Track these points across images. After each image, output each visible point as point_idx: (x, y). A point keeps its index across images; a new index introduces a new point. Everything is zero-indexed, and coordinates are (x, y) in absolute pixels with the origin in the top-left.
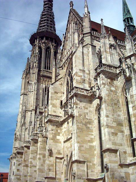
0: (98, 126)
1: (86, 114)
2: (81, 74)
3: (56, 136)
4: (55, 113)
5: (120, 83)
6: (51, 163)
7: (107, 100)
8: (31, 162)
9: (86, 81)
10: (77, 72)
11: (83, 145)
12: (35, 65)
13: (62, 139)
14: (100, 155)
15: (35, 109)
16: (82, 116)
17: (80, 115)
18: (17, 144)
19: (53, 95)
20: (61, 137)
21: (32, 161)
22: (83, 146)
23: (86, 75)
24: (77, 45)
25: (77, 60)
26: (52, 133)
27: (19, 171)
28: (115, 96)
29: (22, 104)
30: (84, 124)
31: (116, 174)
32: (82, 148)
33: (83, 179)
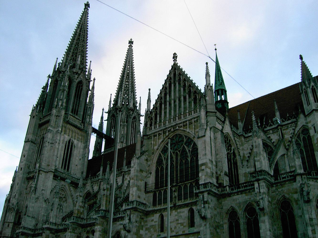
0: (228, 232)
1: (216, 216)
2: (210, 165)
4: (140, 198)
5: (275, 193)
10: (208, 162)
12: (60, 103)
13: (146, 234)
17: (212, 217)
18: (12, 217)
19: (139, 174)
23: (214, 168)
24: (205, 127)
25: (207, 147)
29: (26, 156)
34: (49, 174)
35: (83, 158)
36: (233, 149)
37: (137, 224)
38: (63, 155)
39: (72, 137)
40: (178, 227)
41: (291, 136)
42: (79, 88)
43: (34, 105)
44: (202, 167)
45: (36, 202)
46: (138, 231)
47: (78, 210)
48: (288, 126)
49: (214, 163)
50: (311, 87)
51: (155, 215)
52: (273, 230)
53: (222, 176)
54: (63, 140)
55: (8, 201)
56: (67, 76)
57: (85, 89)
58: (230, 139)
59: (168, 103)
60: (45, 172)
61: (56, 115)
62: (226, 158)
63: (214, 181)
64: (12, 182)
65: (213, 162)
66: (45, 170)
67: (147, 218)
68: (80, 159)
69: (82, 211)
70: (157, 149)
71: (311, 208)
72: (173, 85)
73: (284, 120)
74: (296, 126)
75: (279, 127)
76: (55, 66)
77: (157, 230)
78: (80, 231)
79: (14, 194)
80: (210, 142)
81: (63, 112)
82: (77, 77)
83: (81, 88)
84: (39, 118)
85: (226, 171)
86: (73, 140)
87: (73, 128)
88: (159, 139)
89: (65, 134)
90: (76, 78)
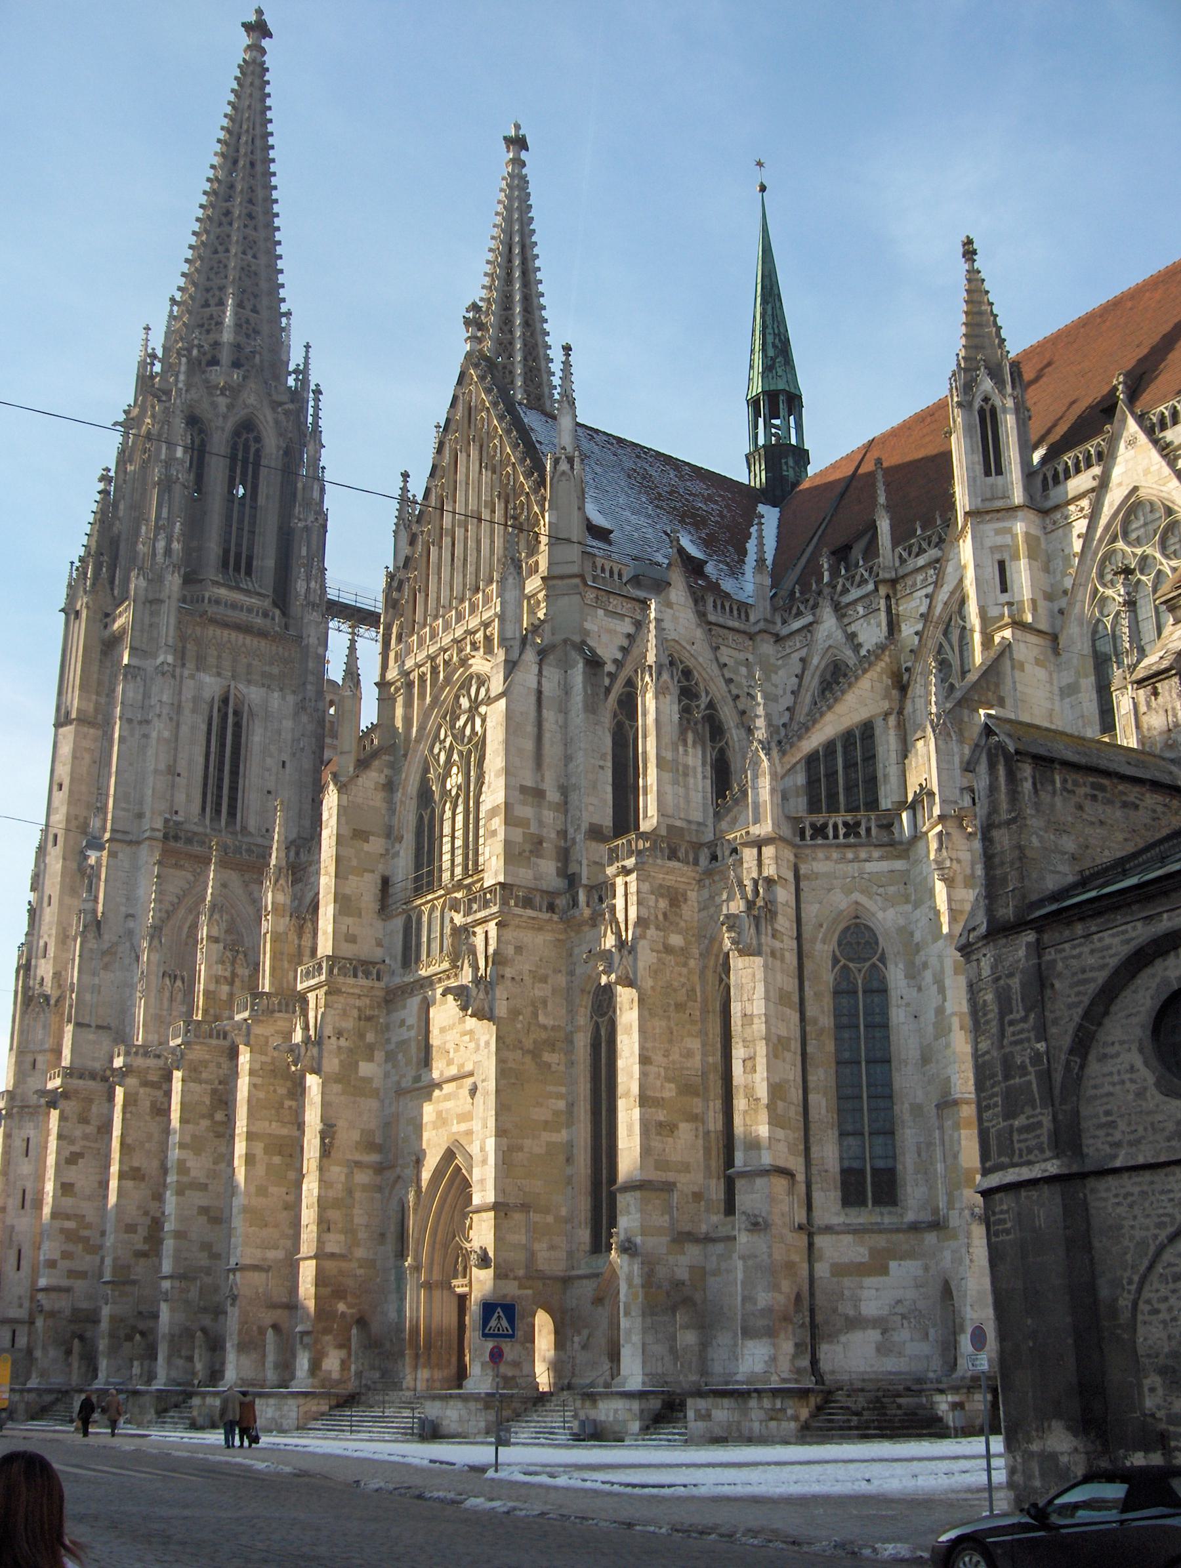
2: (525, 811)
3: (357, 1063)
6: (331, 1194)
7: (649, 992)
8: (181, 1163)
9: (545, 845)
11: (520, 1141)
13: (387, 1075)
14: (589, 1183)
15: (160, 835)
16: (521, 1018)
17: (514, 1013)
20: (380, 1065)
21: (185, 1160)
22: (520, 1148)
23: (549, 816)
24: (515, 655)
26: (339, 1048)
27: (74, 1195)
28: (680, 975)
29: (66, 787)
30: (529, 1052)
31: (661, 1272)
32: (519, 1157)
33: (515, 1278)
34: (145, 847)
35: (294, 754)
36: (703, 706)
37: (342, 1042)
38: (201, 760)
39: (234, 677)
40: (462, 1048)
41: (919, 627)
42: (246, 448)
43: (72, 563)
44: (493, 821)
45: (106, 967)
46: (350, 1066)
47: (207, 993)
48: (915, 584)
49: (553, 795)
50: (977, 403)
51: (409, 1001)
52: (675, 1056)
53: (577, 847)
54: (196, 700)
55: (25, 968)
56: (178, 412)
57: (274, 451)
58: (691, 663)
59: (446, 541)
60: (130, 843)
61: (150, 597)
62: (602, 767)
63: (548, 867)
64: (31, 896)
65: (548, 793)
66: (129, 837)
67: (389, 1013)
68: (284, 763)
69: (224, 997)
70: (418, 740)
71: (754, 976)
72: (461, 457)
73: (905, 555)
74: (936, 583)
75: (883, 591)
76: (143, 365)
77: (414, 1060)
78: (221, 1071)
79: (42, 943)
80: (533, 714)
81: (173, 582)
82: (230, 407)
83: (252, 450)
84: (99, 616)
85: (596, 820)
86: (241, 687)
87: (234, 635)
88: (422, 696)
89: (198, 669)
90: (225, 409)
